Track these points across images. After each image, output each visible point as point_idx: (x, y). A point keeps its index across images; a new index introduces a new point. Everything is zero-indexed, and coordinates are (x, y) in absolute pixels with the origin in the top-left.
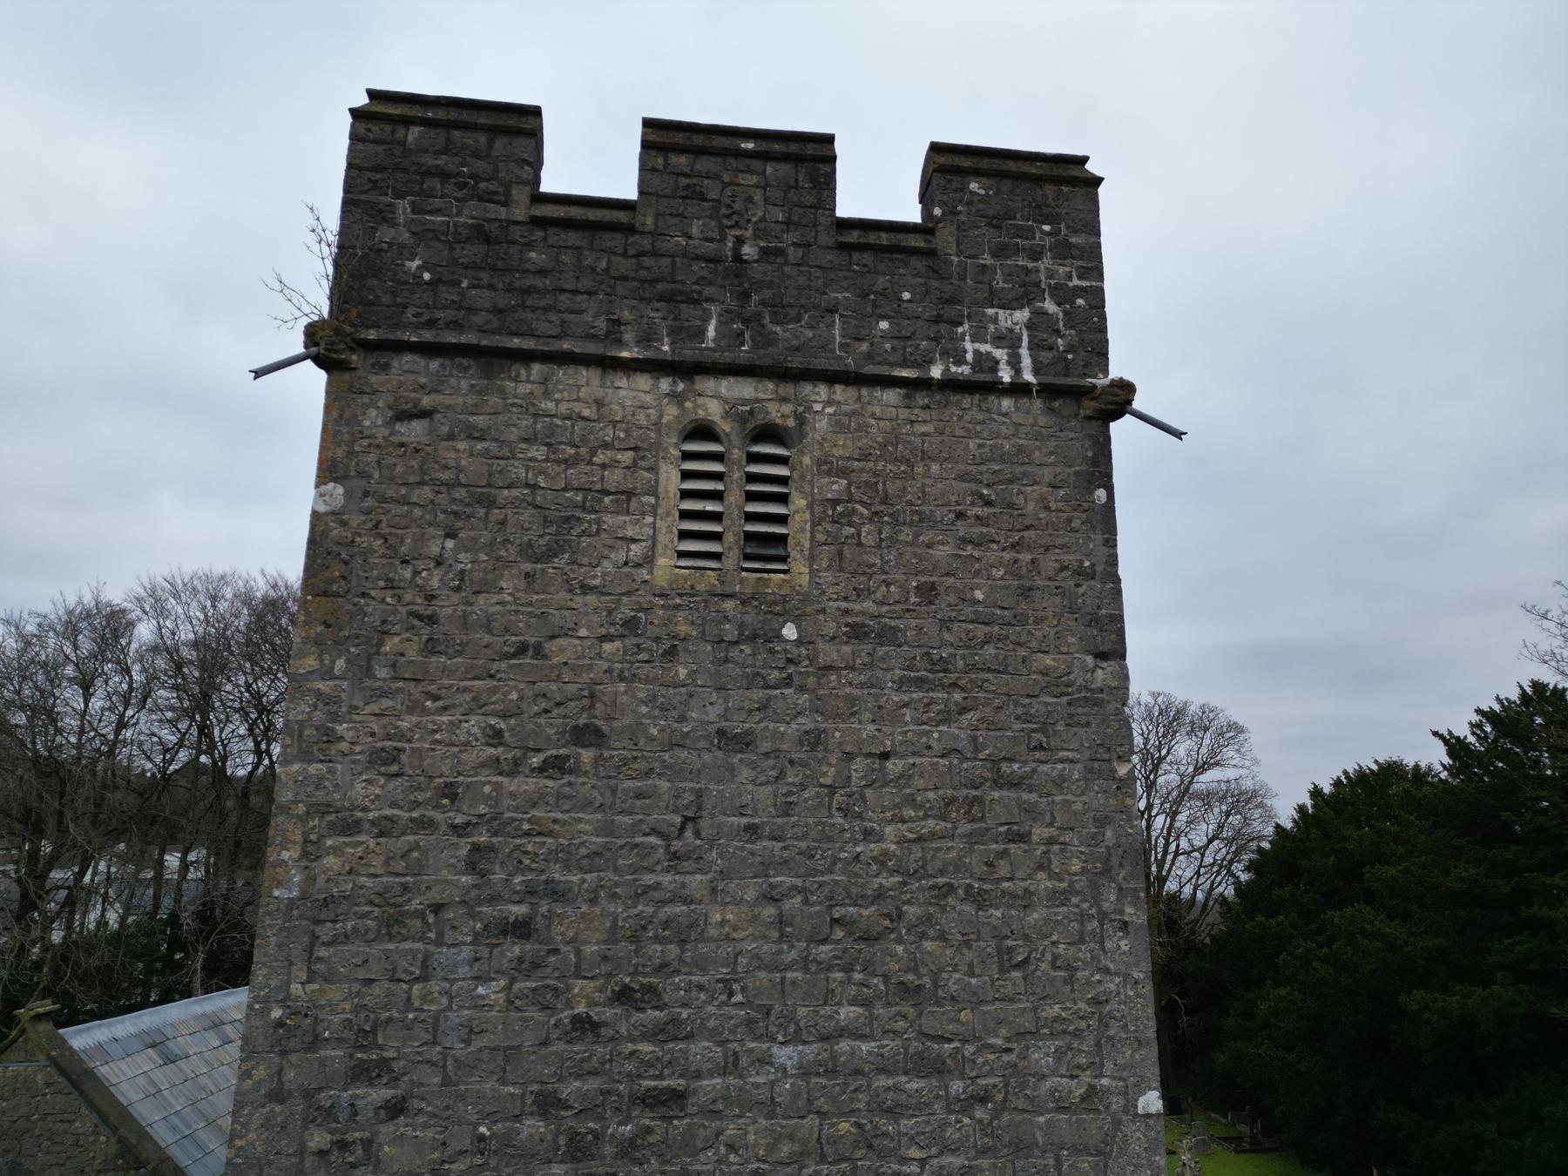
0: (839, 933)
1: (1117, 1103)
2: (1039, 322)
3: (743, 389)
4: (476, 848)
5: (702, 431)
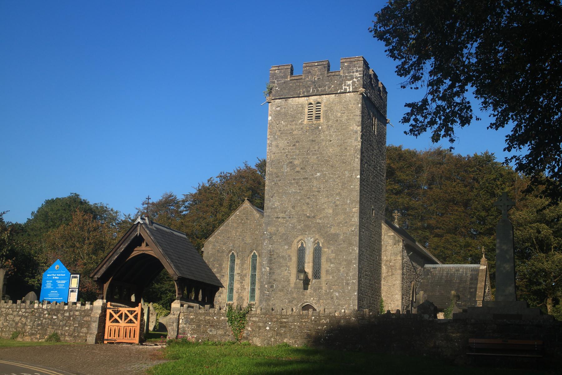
0: (325, 161)
1: (354, 177)
2: (354, 82)
4: (286, 155)
5: (311, 104)
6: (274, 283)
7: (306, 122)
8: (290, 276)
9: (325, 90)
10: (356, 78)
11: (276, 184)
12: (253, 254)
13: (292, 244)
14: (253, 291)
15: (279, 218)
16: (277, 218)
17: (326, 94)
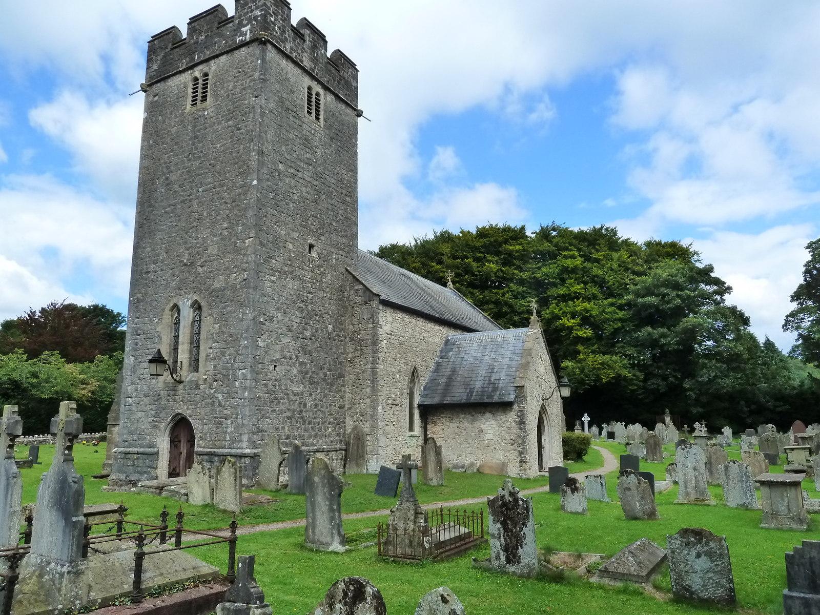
10: (256, 18)
13: (162, 315)
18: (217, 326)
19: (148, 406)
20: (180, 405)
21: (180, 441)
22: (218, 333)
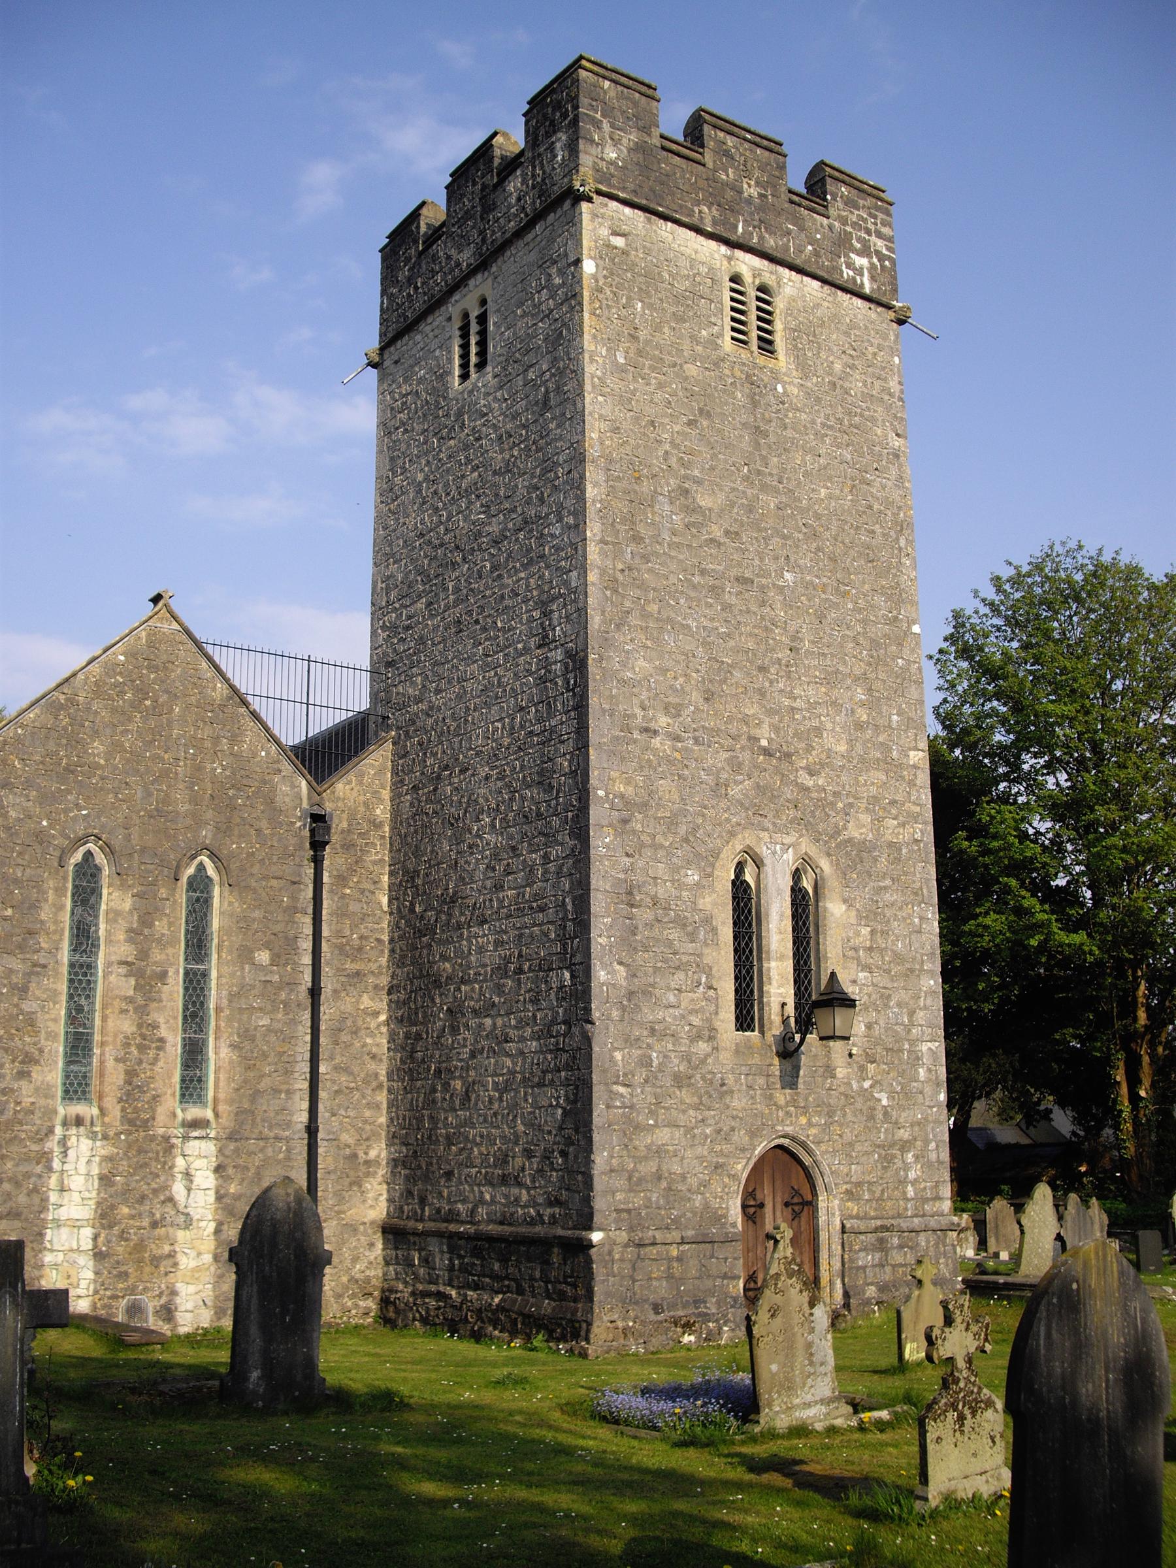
2: (872, 267)
3: (756, 262)
6: (649, 1047)
7: (727, 344)
8: (717, 1013)
9: (787, 249)
11: (630, 569)
12: (191, 871)
13: (714, 866)
14: (194, 1054)
15: (655, 732)
16: (646, 730)
17: (792, 267)
18: (865, 931)
19: (691, 1112)
20: (788, 1114)
21: (762, 1205)
22: (870, 949)
